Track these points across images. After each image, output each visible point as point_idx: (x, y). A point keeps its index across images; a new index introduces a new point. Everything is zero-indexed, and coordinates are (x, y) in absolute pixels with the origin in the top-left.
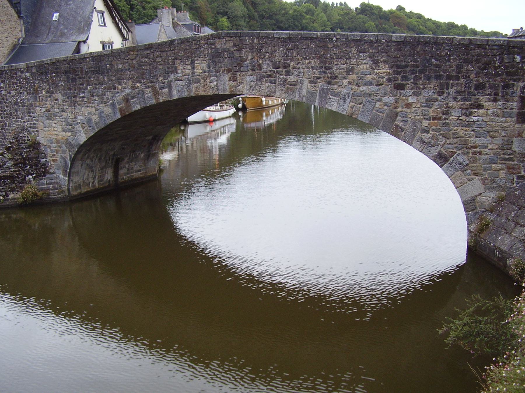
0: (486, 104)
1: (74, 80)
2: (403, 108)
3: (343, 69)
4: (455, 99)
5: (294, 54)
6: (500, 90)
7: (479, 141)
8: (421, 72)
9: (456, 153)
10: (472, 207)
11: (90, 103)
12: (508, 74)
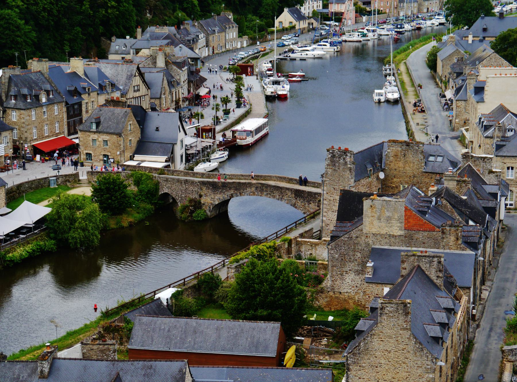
1: (215, 187)
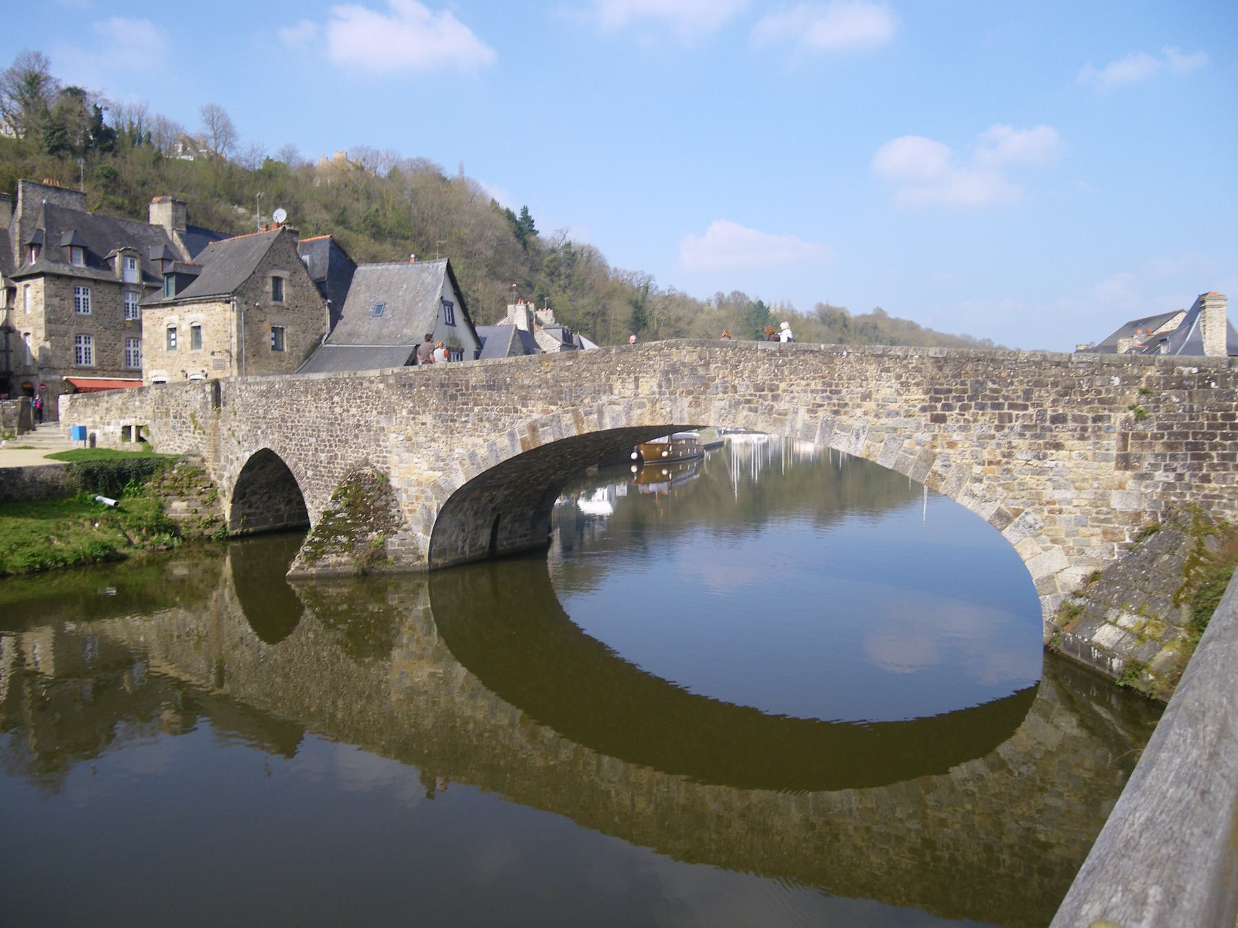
0: (1068, 444)
1: (454, 397)
2: (943, 448)
3: (857, 393)
4: (1022, 435)
5: (786, 373)
6: (1090, 423)
7: (1057, 495)
8: (970, 398)
9: (1023, 511)
10: (1051, 589)
11: (476, 430)
12: (1101, 401)
